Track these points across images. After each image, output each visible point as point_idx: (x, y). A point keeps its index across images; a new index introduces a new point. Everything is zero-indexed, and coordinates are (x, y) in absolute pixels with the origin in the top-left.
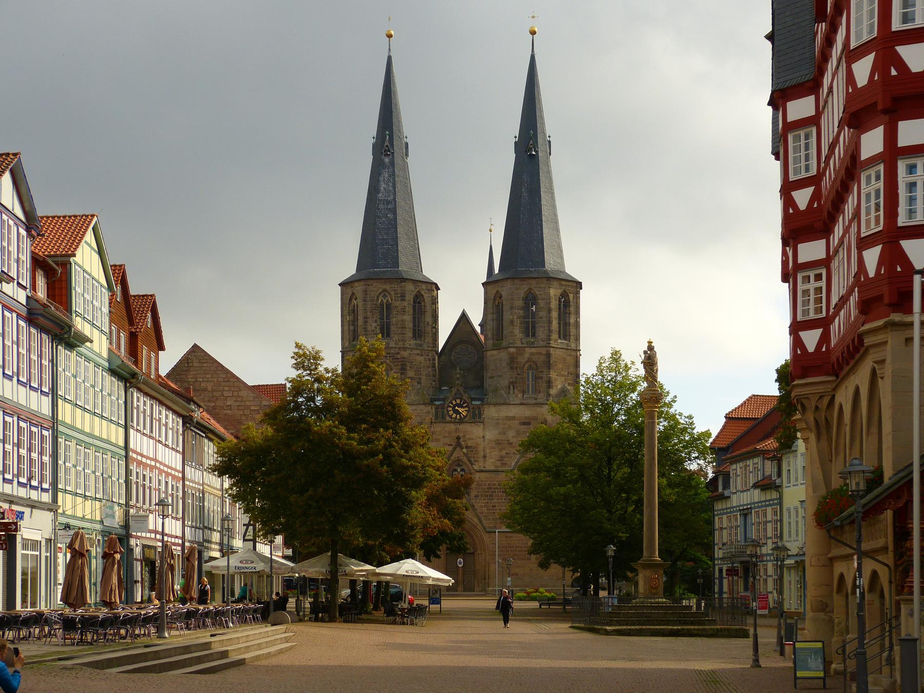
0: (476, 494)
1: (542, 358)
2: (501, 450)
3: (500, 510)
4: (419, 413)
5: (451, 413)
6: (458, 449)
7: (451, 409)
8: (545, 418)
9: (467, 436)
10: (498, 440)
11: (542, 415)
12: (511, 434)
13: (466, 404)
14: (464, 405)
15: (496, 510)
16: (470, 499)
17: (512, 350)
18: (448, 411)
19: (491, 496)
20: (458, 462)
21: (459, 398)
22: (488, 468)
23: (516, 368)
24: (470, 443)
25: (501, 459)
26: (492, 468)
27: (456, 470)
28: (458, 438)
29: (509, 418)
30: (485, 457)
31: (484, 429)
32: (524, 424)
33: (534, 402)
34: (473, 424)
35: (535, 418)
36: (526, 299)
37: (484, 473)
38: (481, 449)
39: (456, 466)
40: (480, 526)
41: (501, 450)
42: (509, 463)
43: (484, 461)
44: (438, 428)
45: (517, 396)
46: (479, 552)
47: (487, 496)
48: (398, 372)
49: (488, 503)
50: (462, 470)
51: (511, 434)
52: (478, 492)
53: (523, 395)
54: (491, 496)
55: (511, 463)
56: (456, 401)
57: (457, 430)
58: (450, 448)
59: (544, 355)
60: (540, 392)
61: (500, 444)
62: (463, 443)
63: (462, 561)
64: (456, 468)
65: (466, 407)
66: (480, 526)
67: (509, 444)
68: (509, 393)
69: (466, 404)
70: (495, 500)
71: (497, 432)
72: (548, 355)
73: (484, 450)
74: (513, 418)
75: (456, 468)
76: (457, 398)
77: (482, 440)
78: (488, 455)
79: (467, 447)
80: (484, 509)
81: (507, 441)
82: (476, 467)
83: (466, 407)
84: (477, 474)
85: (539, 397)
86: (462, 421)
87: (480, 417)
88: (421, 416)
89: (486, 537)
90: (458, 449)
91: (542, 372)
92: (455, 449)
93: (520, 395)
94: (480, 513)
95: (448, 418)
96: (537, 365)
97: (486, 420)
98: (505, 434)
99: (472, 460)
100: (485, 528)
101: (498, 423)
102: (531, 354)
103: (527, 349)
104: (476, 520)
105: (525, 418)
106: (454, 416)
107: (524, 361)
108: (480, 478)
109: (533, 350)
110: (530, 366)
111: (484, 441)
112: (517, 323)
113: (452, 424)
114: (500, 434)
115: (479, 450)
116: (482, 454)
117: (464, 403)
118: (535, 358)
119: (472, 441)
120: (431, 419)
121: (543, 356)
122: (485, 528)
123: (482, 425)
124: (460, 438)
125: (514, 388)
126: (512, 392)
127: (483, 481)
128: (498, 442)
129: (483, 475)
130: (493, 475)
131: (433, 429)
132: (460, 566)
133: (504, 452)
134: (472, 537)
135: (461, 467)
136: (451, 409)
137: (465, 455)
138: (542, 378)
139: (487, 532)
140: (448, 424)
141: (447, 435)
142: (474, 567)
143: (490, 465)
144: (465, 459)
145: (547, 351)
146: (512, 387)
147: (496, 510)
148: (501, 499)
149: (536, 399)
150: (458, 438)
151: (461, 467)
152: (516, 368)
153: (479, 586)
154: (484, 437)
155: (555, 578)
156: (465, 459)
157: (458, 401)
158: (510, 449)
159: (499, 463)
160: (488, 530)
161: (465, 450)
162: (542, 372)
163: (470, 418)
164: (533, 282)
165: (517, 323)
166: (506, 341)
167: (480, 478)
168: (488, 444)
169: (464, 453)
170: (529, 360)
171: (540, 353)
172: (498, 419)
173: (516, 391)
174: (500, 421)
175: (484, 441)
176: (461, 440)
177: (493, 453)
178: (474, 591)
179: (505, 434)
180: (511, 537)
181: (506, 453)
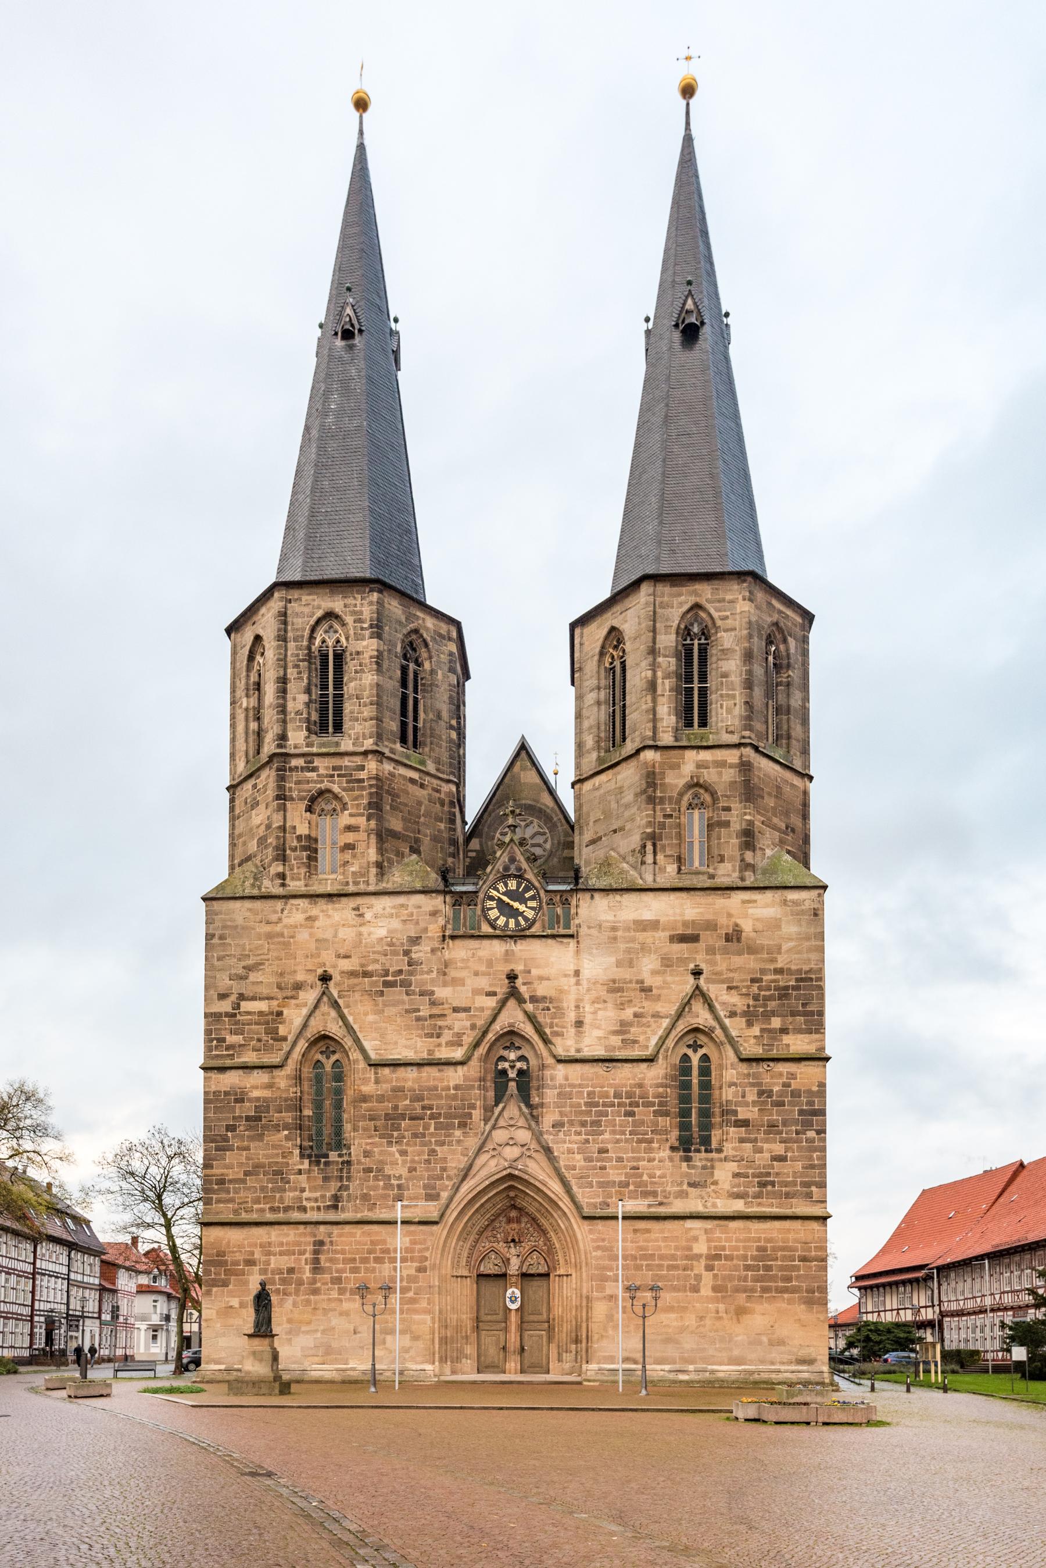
0: (557, 1117)
1: (729, 775)
2: (621, 1006)
3: (620, 1159)
4: (412, 914)
5: (494, 914)
6: (512, 1003)
7: (493, 904)
8: (737, 925)
9: (534, 972)
10: (614, 981)
11: (730, 915)
12: (647, 966)
13: (531, 893)
14: (527, 895)
15: (610, 1160)
16: (541, 1133)
17: (649, 755)
18: (485, 911)
19: (594, 1123)
20: (511, 1037)
21: (515, 876)
22: (587, 1053)
23: (662, 800)
24: (541, 990)
25: (623, 1027)
26: (600, 1052)
27: (502, 1058)
28: (512, 977)
29: (643, 926)
30: (579, 1024)
31: (578, 952)
32: (683, 939)
33: (708, 883)
34: (550, 941)
35: (711, 926)
36: (685, 633)
37: (578, 1067)
38: (569, 1003)
39: (506, 1048)
40: (565, 1204)
41: (621, 1006)
42: (641, 1038)
43: (579, 1034)
44: (459, 951)
45: (663, 870)
46: (561, 1272)
47: (583, 1124)
48: (362, 815)
49: (587, 1141)
50: (522, 1058)
51: (647, 966)
52: (561, 1114)
53: (679, 869)
54: (597, 1123)
55: (648, 1039)
56: (506, 885)
57: (508, 955)
58: (491, 1002)
59: (731, 766)
60: (722, 860)
61: (620, 990)
62: (523, 989)
63: (518, 1293)
64: (505, 1053)
65: (532, 898)
66: (565, 1204)
67: (643, 990)
68: (643, 863)
69: (531, 893)
70: (607, 1136)
71: (613, 959)
72: (745, 767)
73: (577, 1007)
74: (654, 925)
75: (505, 1053)
76: (509, 876)
77: (573, 980)
78: (588, 1020)
79: (534, 999)
80: (579, 1157)
81: (637, 982)
82: (560, 1051)
83: (532, 898)
84: (560, 1067)
85: (720, 872)
86: (519, 935)
87: (567, 926)
88: (417, 923)
89: (582, 1231)
90: (512, 1003)
91: (728, 809)
92: (503, 1003)
93: (672, 868)
94: (568, 1167)
95: (486, 929)
96: (713, 794)
97: (583, 931)
98: (631, 964)
99: (548, 1031)
100: (578, 1207)
101: (615, 938)
102: (700, 765)
103: (691, 755)
104: (555, 1187)
105: (685, 924)
106: (502, 921)
107: (681, 782)
108: (567, 1079)
109: (705, 755)
110: (696, 796)
111: (578, 983)
112: (664, 690)
113: (496, 943)
114: (619, 964)
115: (565, 1005)
116: (571, 1016)
117: (527, 889)
118: (709, 776)
119: (545, 983)
120: (444, 928)
121: (732, 771)
122: (578, 1207)
123: (572, 943)
124: (515, 977)
125: (655, 853)
126: (649, 858)
127: (570, 1085)
128: (615, 987)
129: (576, 1071)
130: (599, 1069)
131: (447, 955)
132: (514, 1307)
133: (628, 1013)
134: (544, 1232)
135: (520, 1053)
136: (493, 904)
137: (531, 1018)
138: (727, 824)
139: (585, 1218)
140: (486, 943)
141: (483, 968)
142: (549, 1310)
143: (592, 1044)
144: (529, 1030)
145: (741, 756)
146: (649, 847)
147: (610, 1160)
148: (623, 1133)
149: (712, 877)
150: (512, 977)
151: (520, 1053)
152: (662, 800)
153: (560, 1360)
154: (577, 973)
155: (765, 1339)
156: (529, 1030)
157: (512, 884)
158: (646, 1004)
159: (616, 1040)
160: (587, 1211)
161: (529, 1007)
162: (728, 809)
163: (544, 927)
164: (705, 592)
165: (664, 690)
166: (633, 741)
167: (567, 1079)
168: (588, 990)
169: (526, 1012)
170: (695, 784)
171: (722, 764)
172: (614, 929)
173: (660, 857)
174: (619, 933)
175: (578, 983)
176: (519, 982)
177: (600, 1013)
178: (548, 1372)
179: (631, 964)
180: (648, 1231)
181: (636, 1015)
